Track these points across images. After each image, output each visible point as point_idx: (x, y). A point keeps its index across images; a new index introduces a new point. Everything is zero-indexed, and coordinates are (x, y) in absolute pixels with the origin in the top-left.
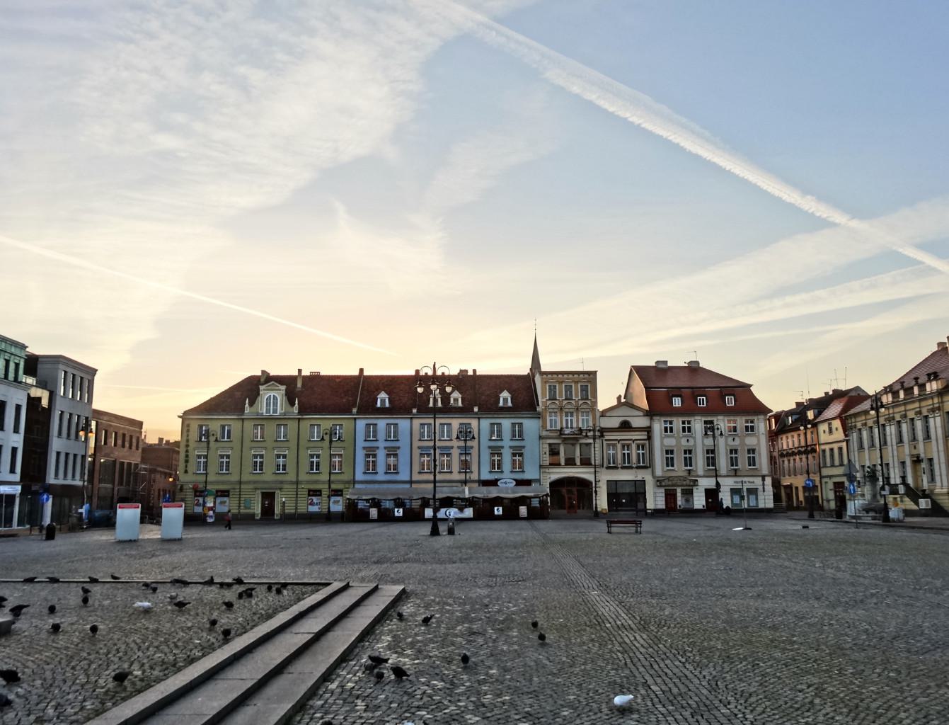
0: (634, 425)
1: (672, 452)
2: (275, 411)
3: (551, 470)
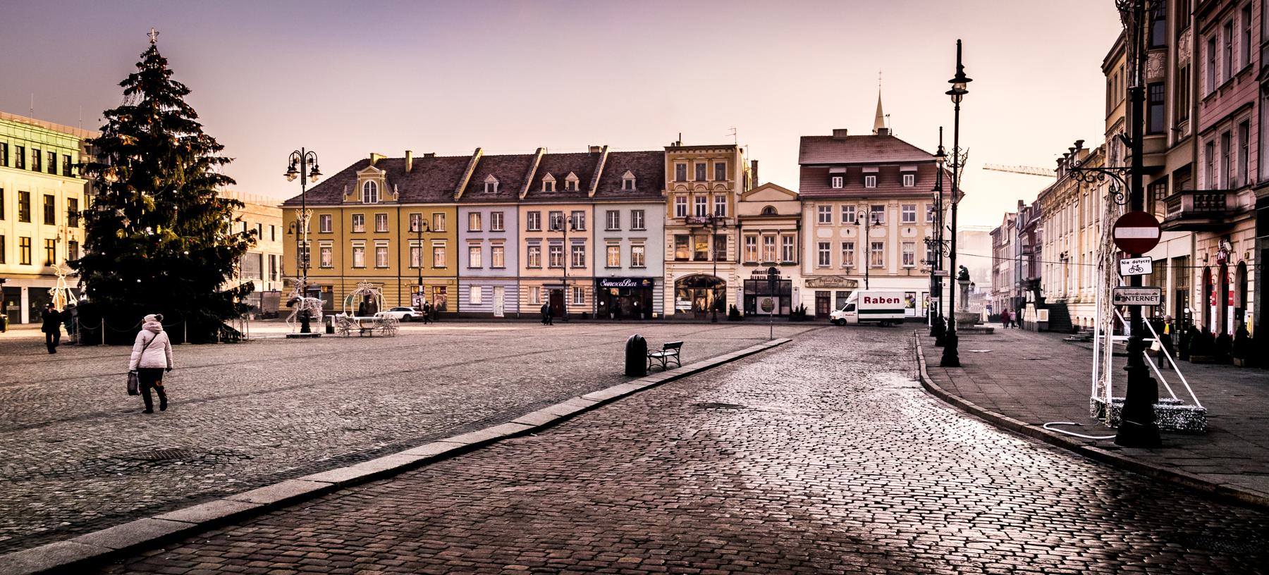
0: (782, 209)
1: (828, 246)
2: (374, 199)
3: (677, 266)
